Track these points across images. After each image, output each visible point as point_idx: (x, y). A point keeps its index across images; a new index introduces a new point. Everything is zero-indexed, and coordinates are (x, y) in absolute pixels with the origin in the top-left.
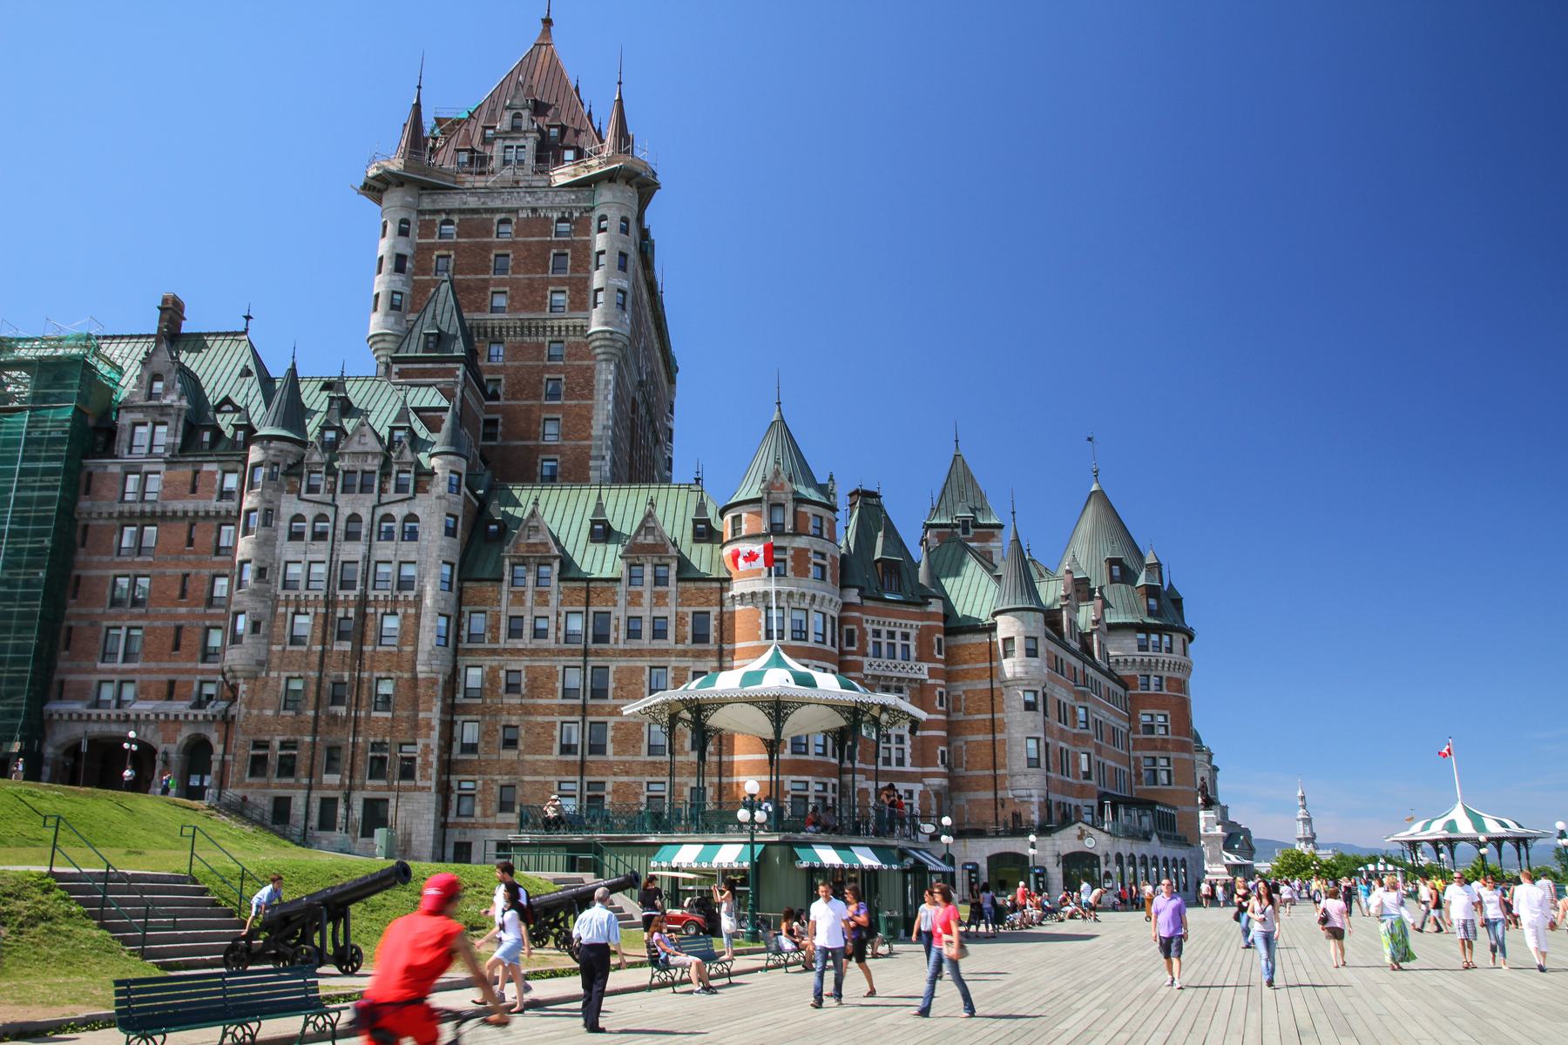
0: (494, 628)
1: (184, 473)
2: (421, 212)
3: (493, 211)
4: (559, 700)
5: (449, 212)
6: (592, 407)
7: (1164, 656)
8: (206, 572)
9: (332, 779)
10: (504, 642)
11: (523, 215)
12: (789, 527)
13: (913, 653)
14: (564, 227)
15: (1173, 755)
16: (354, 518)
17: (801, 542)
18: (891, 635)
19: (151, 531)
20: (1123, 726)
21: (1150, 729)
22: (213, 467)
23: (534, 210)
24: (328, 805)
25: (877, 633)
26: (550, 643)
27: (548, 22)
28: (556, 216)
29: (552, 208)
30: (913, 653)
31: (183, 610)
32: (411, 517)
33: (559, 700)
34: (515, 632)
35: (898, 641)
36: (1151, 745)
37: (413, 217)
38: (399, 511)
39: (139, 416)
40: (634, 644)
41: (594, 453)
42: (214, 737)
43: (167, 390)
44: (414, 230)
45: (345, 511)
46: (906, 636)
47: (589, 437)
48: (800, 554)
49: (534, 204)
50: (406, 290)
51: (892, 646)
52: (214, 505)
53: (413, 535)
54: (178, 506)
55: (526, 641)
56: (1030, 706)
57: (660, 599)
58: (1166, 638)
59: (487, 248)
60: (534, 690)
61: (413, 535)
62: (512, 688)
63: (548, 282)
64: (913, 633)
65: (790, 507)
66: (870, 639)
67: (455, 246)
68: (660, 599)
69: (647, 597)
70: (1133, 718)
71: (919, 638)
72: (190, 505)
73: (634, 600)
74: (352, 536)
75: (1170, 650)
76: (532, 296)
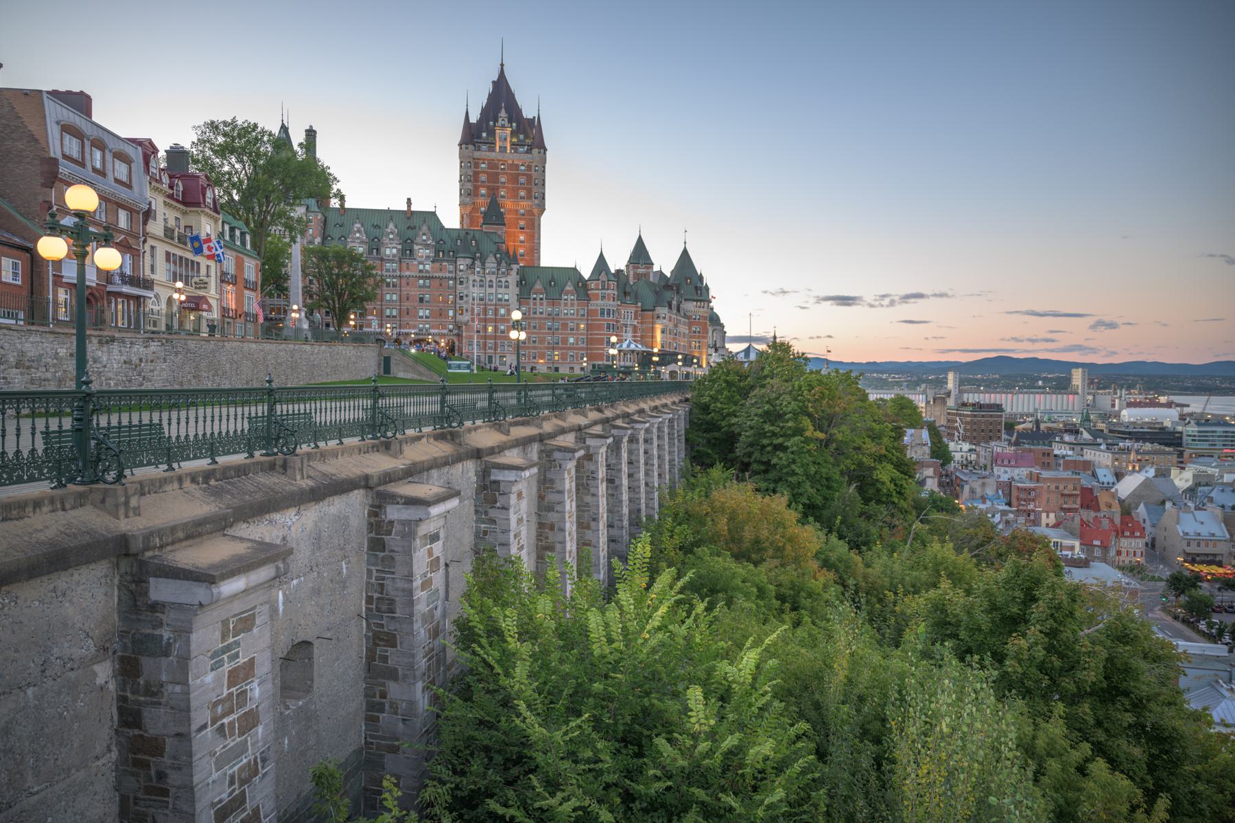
0: (529, 311)
1: (437, 265)
7: (701, 309)
10: (532, 315)
11: (510, 162)
14: (523, 168)
16: (491, 281)
17: (610, 291)
19: (427, 281)
20: (687, 332)
21: (695, 332)
24: (490, 357)
26: (544, 316)
27: (502, 65)
32: (507, 281)
34: (535, 313)
38: (503, 280)
42: (456, 340)
43: (428, 239)
45: (488, 279)
48: (609, 294)
52: (447, 275)
53: (507, 287)
54: (435, 275)
55: (538, 315)
57: (572, 305)
59: (498, 174)
60: (540, 329)
61: (507, 287)
62: (535, 327)
63: (518, 189)
67: (487, 173)
68: (572, 305)
70: (690, 329)
72: (440, 275)
74: (491, 286)
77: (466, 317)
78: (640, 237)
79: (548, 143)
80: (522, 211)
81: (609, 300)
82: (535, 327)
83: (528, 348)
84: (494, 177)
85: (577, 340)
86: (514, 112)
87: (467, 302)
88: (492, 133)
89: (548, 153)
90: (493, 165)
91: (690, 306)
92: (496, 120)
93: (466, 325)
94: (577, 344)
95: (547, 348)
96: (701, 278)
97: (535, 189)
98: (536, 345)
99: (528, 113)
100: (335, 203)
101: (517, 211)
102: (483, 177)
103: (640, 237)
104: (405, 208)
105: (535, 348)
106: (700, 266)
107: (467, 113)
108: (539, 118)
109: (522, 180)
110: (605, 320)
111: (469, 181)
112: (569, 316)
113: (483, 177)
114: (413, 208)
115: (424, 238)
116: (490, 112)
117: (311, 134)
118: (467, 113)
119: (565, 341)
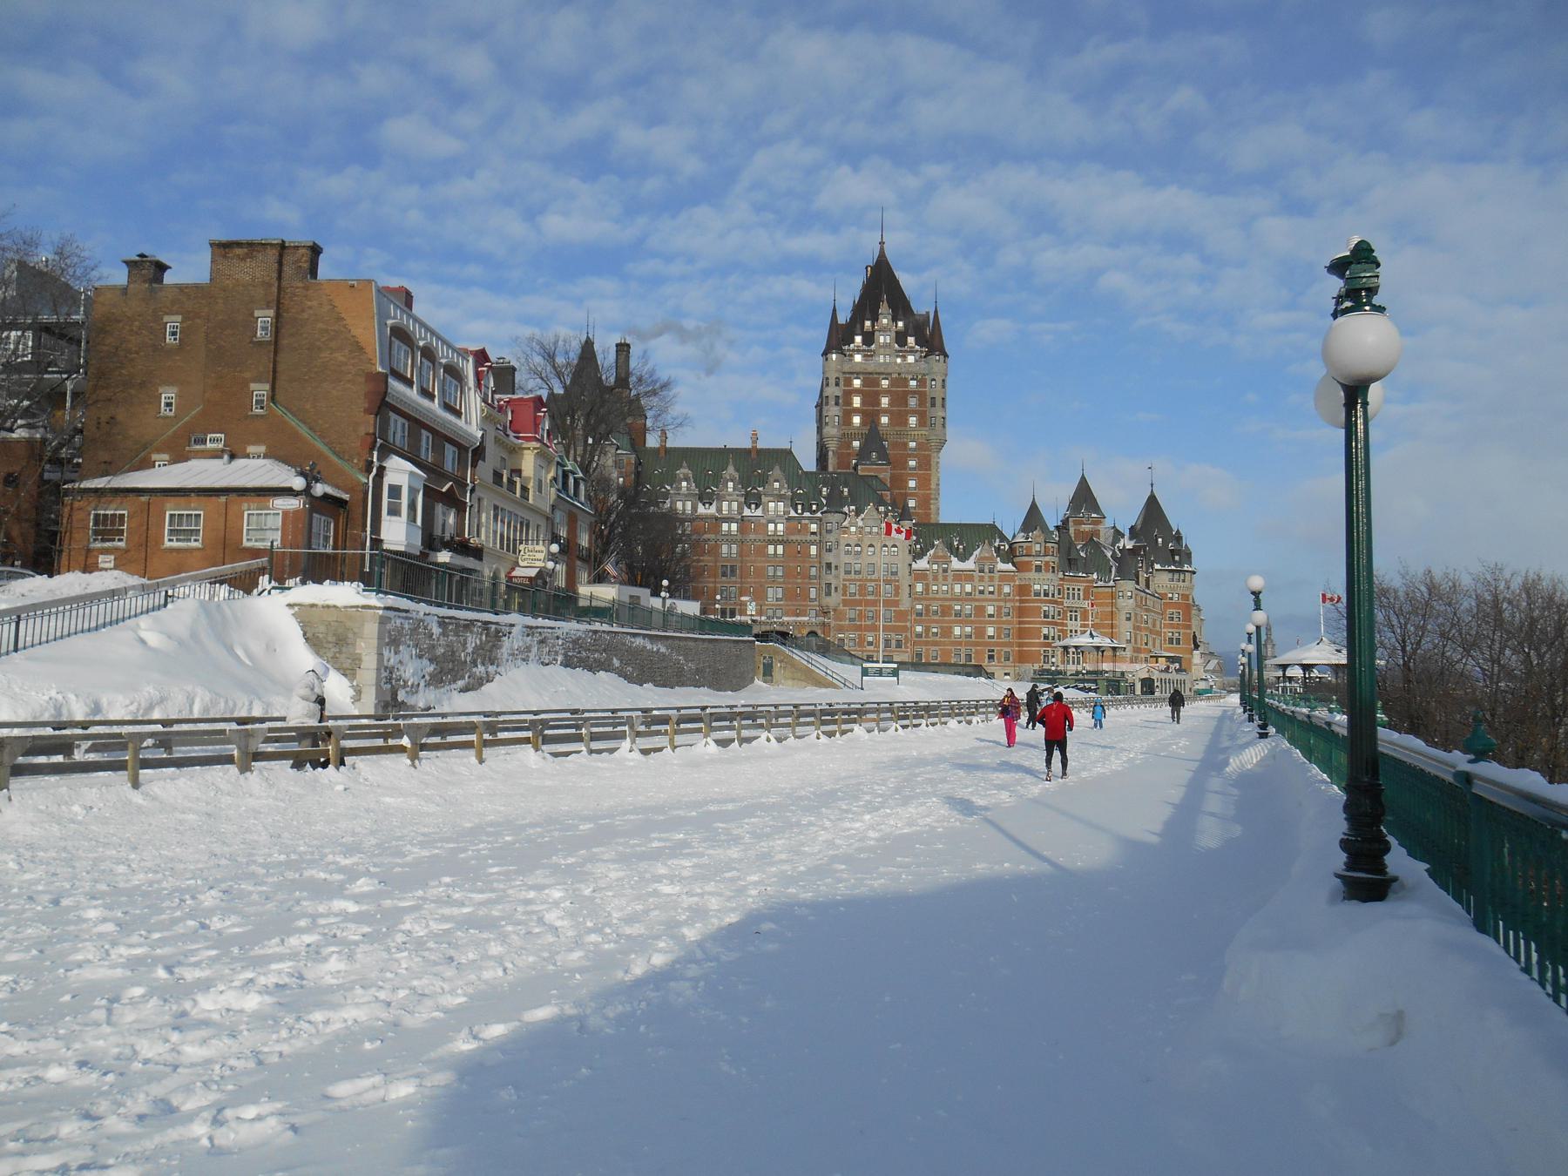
2: (844, 373)
3: (879, 374)
4: (953, 618)
5: (858, 374)
6: (930, 475)
7: (1181, 584)
8: (807, 565)
9: (872, 648)
11: (894, 376)
12: (1043, 551)
13: (1082, 597)
14: (913, 383)
15: (1182, 631)
17: (1047, 559)
18: (1074, 589)
19: (780, 549)
22: (807, 521)
23: (899, 374)
25: (1068, 589)
26: (949, 596)
28: (910, 377)
29: (908, 373)
30: (1082, 597)
31: (799, 581)
33: (953, 618)
35: (1076, 592)
36: (1172, 626)
37: (841, 376)
39: (772, 499)
40: (982, 596)
41: (933, 496)
44: (842, 383)
46: (1079, 590)
47: (930, 489)
48: (1047, 563)
49: (899, 371)
50: (840, 414)
51: (1074, 594)
56: (1129, 619)
58: (1182, 576)
64: (1082, 588)
65: (1043, 544)
66: (1066, 592)
68: (991, 579)
69: (987, 579)
71: (1084, 590)
73: (982, 579)
75: (1184, 581)
76: (899, 418)
77: (834, 600)
78: (1083, 478)
79: (947, 350)
80: (912, 445)
81: (1047, 571)
82: (936, 613)
83: (927, 643)
84: (871, 398)
85: (998, 630)
86: (901, 305)
87: (837, 577)
88: (869, 338)
89: (948, 360)
90: (871, 380)
91: (1162, 581)
92: (875, 319)
93: (835, 610)
94: (999, 637)
95: (953, 643)
96: (1178, 538)
97: (931, 412)
98: (937, 639)
99: (920, 307)
100: (652, 441)
101: (906, 445)
102: (857, 402)
103: (1083, 478)
104: (748, 445)
105: (936, 644)
106: (1175, 520)
107: (834, 310)
108: (936, 312)
109: (913, 402)
110: (1042, 601)
111: (837, 404)
112: (987, 596)
113: (857, 402)
114: (760, 445)
115: (777, 485)
116: (866, 307)
117: (623, 349)
118: (834, 310)
119: (980, 632)
